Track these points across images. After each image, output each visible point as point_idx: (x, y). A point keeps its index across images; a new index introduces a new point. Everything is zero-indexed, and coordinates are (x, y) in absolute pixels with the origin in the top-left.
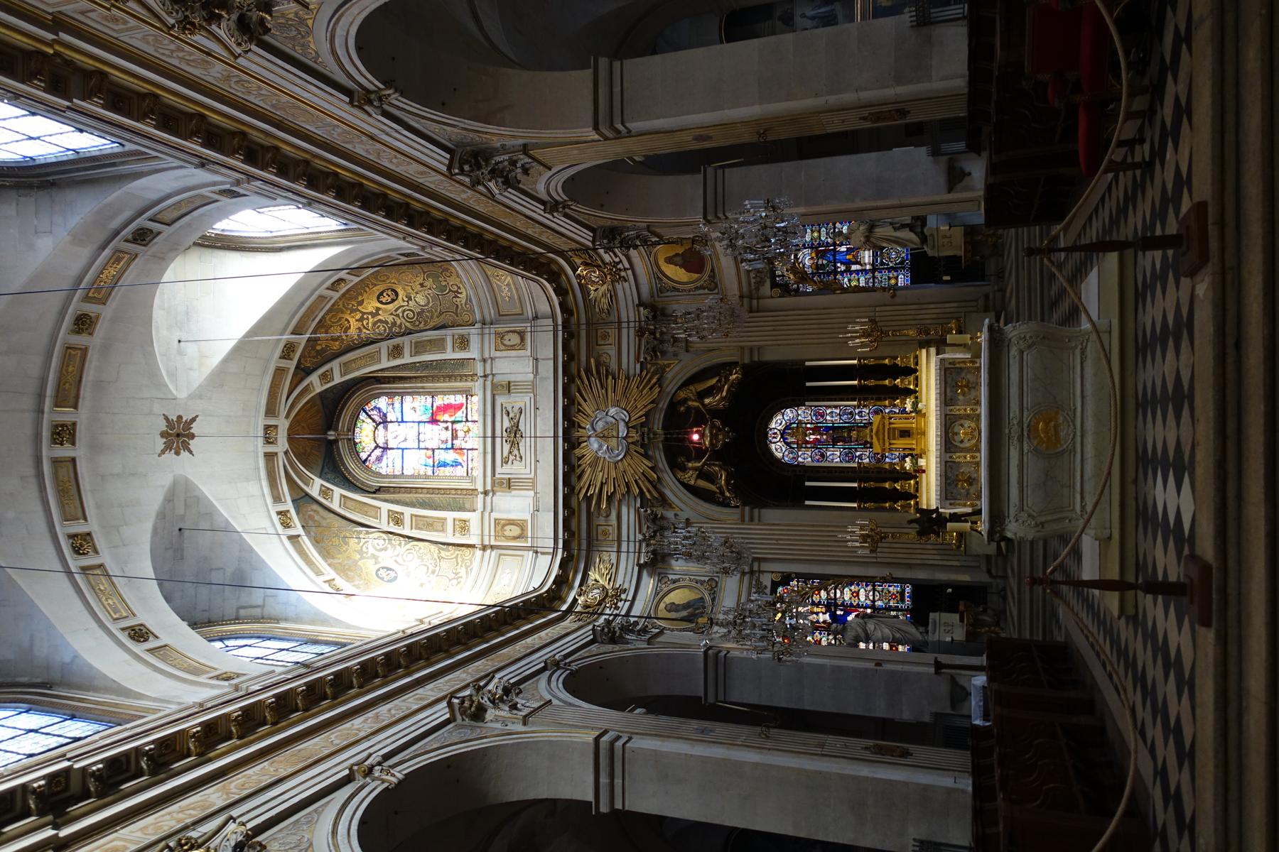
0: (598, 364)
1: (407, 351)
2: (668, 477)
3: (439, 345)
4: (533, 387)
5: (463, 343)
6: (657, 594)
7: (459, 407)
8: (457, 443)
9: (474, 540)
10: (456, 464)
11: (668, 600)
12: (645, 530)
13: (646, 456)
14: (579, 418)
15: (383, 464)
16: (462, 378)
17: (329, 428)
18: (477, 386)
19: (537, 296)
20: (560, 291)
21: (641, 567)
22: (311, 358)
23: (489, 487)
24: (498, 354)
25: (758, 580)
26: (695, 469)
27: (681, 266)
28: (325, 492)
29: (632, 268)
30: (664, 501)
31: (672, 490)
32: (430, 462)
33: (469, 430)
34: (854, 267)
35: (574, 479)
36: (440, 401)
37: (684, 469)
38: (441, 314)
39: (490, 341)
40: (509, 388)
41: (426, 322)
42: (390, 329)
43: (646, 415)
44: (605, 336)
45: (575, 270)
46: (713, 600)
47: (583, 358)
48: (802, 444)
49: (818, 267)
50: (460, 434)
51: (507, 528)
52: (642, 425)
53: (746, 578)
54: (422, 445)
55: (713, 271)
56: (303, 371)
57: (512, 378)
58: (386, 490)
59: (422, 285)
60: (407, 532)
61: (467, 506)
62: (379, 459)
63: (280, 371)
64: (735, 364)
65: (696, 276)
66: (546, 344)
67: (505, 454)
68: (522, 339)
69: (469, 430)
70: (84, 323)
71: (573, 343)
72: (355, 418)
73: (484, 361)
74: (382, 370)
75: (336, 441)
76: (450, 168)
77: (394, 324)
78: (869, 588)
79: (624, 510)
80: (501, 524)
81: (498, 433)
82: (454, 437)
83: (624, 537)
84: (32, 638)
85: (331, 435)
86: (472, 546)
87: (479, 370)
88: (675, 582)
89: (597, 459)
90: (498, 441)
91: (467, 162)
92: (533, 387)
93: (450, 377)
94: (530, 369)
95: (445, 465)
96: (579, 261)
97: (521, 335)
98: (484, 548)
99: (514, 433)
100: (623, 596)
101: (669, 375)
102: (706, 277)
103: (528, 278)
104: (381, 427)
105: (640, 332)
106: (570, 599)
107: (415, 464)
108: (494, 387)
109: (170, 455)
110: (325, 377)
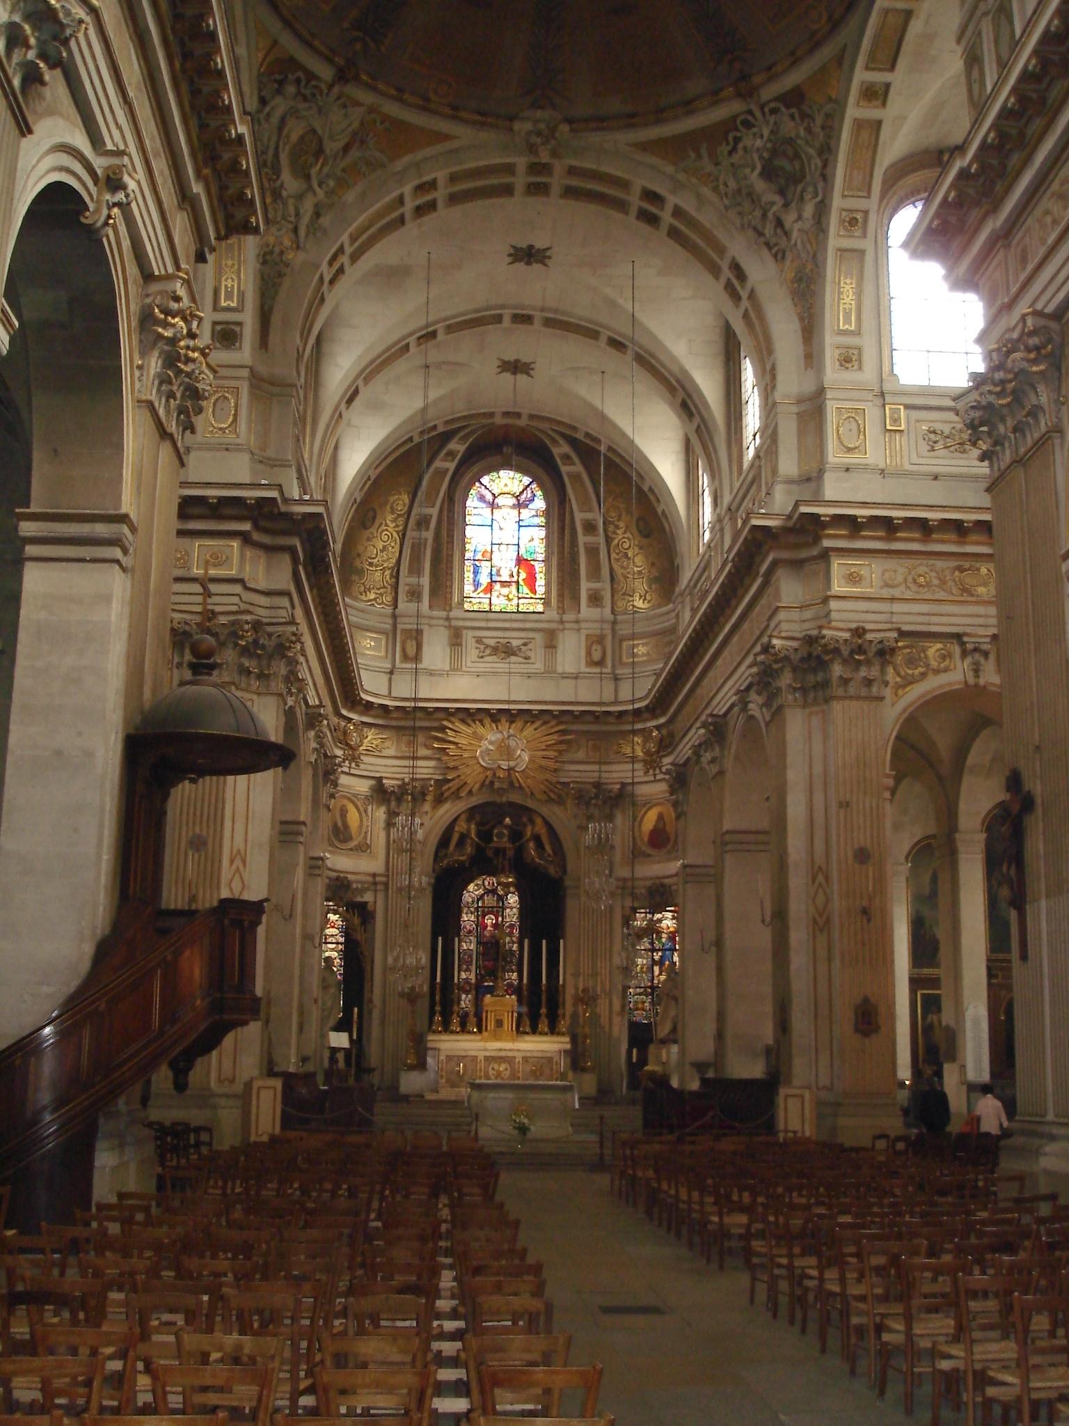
0: (569, 742)
1: (590, 539)
3: (595, 574)
5: (595, 599)
6: (355, 795)
9: (401, 605)
10: (477, 585)
13: (483, 785)
14: (519, 724)
15: (477, 503)
16: (561, 596)
18: (553, 614)
19: (638, 690)
20: (637, 713)
21: (380, 779)
22: (587, 451)
23: (454, 623)
24: (583, 638)
26: (469, 830)
27: (655, 826)
28: (451, 454)
29: (655, 781)
30: (439, 800)
32: (479, 556)
33: (509, 600)
34: (656, 969)
35: (461, 715)
36: (539, 567)
37: (469, 821)
39: (594, 629)
40: (551, 646)
41: (618, 560)
42: (612, 523)
43: (521, 787)
44: (596, 748)
45: (657, 727)
46: (351, 849)
47: (575, 727)
48: (482, 912)
50: (505, 591)
52: (511, 784)
53: (370, 879)
55: (649, 855)
56: (573, 442)
57: (559, 651)
58: (451, 510)
60: (408, 533)
62: (482, 498)
63: (574, 429)
64: (565, 872)
65: (646, 839)
66: (589, 694)
67: (486, 641)
69: (509, 600)
70: (617, 345)
71: (589, 718)
72: (525, 472)
73: (577, 622)
74: (572, 512)
75: (501, 452)
77: (617, 527)
79: (432, 763)
80: (417, 636)
81: (507, 634)
82: (505, 584)
85: (507, 450)
86: (396, 607)
88: (366, 811)
89: (480, 739)
90: (499, 634)
92: (549, 672)
93: (561, 584)
94: (565, 678)
95: (476, 573)
96: (664, 732)
97: (600, 663)
98: (394, 616)
99: (506, 651)
100: (353, 765)
101: (557, 810)
102: (644, 848)
104: (514, 501)
105: (597, 785)
106: (351, 715)
107: (476, 537)
110: (566, 458)
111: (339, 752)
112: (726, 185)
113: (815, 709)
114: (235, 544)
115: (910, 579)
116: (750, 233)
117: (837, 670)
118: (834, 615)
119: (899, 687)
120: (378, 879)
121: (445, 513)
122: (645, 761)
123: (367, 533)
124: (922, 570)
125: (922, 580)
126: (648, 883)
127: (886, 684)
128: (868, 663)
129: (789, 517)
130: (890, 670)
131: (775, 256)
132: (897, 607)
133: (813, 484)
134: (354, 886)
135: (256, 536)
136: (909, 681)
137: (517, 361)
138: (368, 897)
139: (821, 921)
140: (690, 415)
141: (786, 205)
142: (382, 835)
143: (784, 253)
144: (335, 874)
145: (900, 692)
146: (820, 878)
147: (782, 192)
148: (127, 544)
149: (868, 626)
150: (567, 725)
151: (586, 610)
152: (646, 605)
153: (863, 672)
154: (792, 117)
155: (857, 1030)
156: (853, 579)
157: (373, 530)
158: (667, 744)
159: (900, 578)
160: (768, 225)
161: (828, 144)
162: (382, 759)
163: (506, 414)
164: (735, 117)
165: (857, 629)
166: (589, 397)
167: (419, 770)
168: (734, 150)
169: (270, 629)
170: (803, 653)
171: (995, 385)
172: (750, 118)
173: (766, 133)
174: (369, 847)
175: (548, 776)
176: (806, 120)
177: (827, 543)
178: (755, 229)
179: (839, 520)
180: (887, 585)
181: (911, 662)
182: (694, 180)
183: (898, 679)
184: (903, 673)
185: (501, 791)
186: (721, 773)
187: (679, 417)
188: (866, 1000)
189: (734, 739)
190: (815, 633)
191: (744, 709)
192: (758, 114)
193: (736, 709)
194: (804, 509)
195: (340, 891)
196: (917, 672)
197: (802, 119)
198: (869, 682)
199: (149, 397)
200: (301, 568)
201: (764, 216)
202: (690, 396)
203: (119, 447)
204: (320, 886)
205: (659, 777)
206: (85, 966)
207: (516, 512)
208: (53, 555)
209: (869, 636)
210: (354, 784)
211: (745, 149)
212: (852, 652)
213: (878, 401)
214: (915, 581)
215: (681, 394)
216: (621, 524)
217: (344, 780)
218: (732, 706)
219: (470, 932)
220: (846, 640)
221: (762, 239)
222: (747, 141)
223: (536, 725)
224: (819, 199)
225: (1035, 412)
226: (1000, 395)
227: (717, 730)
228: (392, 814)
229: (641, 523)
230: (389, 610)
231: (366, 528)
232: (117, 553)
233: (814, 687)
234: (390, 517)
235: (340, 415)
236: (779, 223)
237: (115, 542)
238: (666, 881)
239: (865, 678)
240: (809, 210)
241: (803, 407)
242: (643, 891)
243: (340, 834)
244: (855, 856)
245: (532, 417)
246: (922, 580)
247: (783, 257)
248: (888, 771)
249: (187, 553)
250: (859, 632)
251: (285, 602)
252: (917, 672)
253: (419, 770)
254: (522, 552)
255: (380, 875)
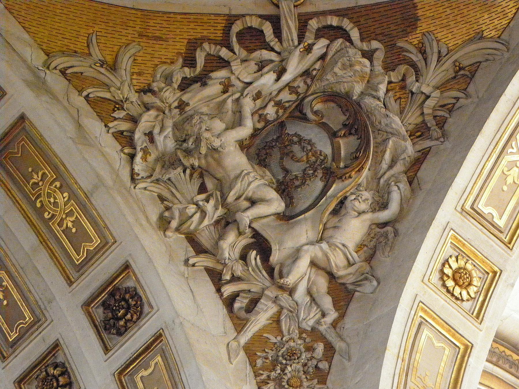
112: (150, 136)
116: (176, 239)
131: (229, 303)
141: (287, 217)
143: (254, 303)
147: (284, 189)
154: (369, 55)
160: (231, 237)
161: (441, 123)
164: (231, 19)
168: (202, 80)
172: (268, 29)
173: (294, 67)
176: (403, 68)
178: (192, 240)
182: (79, 101)
192: (290, 27)
197: (389, 67)
201: (226, 223)
211: (227, 87)
221: (203, 261)
222: (243, 72)
224: (384, 215)
236: (261, 245)
240: (354, 230)
247: (252, 306)
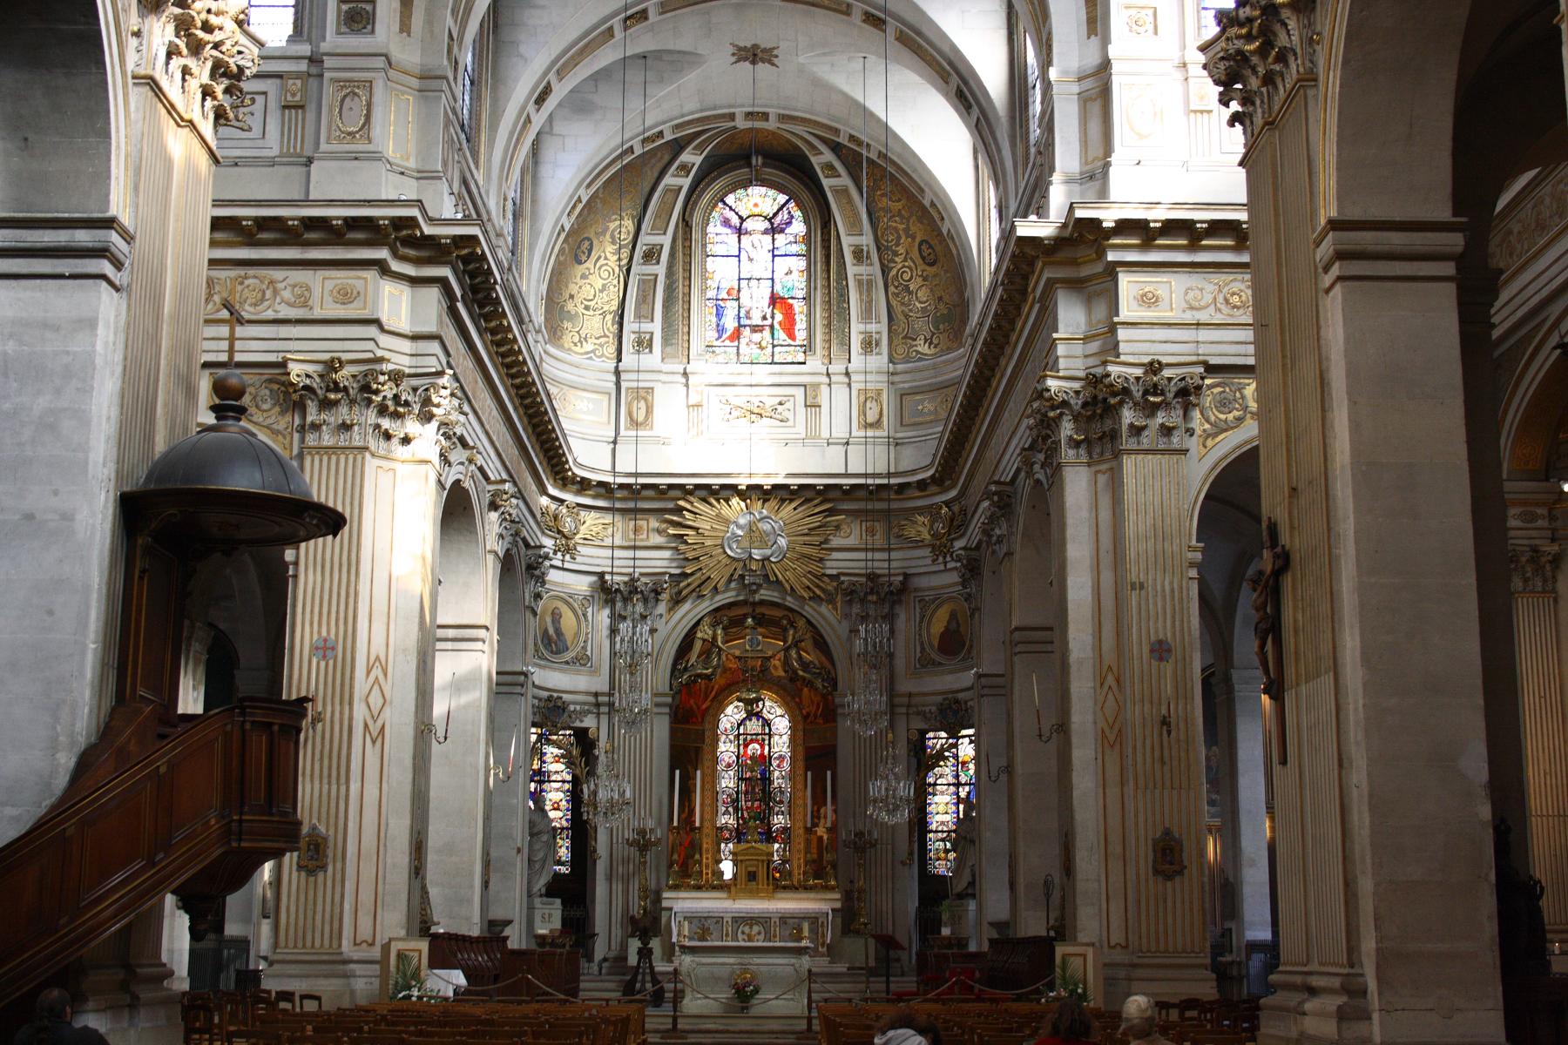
1: (862, 269)
2: (706, 606)
3: (867, 315)
4: (811, 437)
7: (792, 336)
8: (747, 332)
9: (628, 359)
11: (564, 609)
12: (644, 580)
14: (773, 503)
17: (765, 156)
20: (922, 485)
21: (601, 575)
22: (850, 156)
25: (590, 712)
26: (714, 637)
27: (947, 628)
28: (685, 169)
29: (946, 570)
30: (677, 601)
31: (690, 611)
32: (723, 295)
35: (703, 493)
37: (714, 626)
38: (907, 317)
41: (897, 295)
42: (887, 248)
43: (778, 581)
44: (872, 532)
45: (947, 503)
48: (743, 741)
49: (964, 763)
50: (757, 337)
51: (642, 404)
53: (591, 699)
54: (744, 283)
55: (940, 664)
56: (836, 148)
58: (688, 237)
59: (940, 299)
61: (668, 349)
62: (726, 222)
63: (837, 131)
68: (871, 425)
69: (762, 348)
70: (875, 21)
72: (781, 190)
76: (998, 483)
77: (896, 254)
78: (565, 824)
79: (667, 554)
80: (644, 395)
82: (756, 329)
83: (640, 554)
84: (543, 7)
85: (757, 161)
86: (619, 360)
87: (838, 367)
91: (1001, 499)
92: (811, 437)
95: (719, 315)
96: (956, 508)
97: (877, 424)
98: (617, 373)
100: (568, 557)
101: (824, 609)
102: (933, 655)
103: (940, 439)
104: (767, 225)
107: (720, 271)
108: (816, 386)
109: (732, 50)
110: (829, 166)
111: (548, 543)
113: (1104, 467)
114: (371, 274)
115: (1220, 299)
117: (1128, 416)
118: (1123, 347)
119: (1208, 435)
120: (601, 699)
121: (680, 242)
122: (933, 546)
123: (580, 269)
124: (1236, 286)
125: (1235, 299)
126: (939, 699)
127: (1190, 432)
128: (1166, 405)
129: (1065, 225)
130: (1196, 414)
132: (1204, 335)
133: (1096, 184)
134: (572, 708)
135: (395, 266)
136: (1220, 429)
137: (755, 46)
138: (589, 722)
139: (1112, 738)
140: (968, 107)
142: (607, 643)
144: (545, 694)
145: (1210, 443)
146: (1110, 680)
148: (121, 257)
149: (1164, 360)
150: (821, 499)
151: (857, 361)
152: (933, 351)
153: (1160, 418)
155: (1156, 872)
156: (1148, 300)
157: (590, 264)
158: (957, 524)
159: (1208, 298)
162: (600, 546)
163: (749, 115)
165: (1151, 364)
166: (847, 89)
167: (638, 563)
169: (415, 382)
170: (1087, 394)
171: (1241, 25)
174: (589, 659)
175: (813, 567)
177: (1111, 256)
179: (1126, 227)
180: (1192, 308)
181: (1223, 405)
183: (1207, 426)
184: (1213, 419)
185: (752, 589)
186: (1009, 554)
187: (957, 110)
188: (1167, 832)
189: (1021, 510)
190: (1099, 371)
191: (1030, 473)
193: (1023, 474)
194: (1079, 214)
195: (551, 713)
196: (1230, 416)
198: (1167, 431)
199: (149, 72)
200: (460, 305)
202: (966, 83)
203: (106, 134)
204: (524, 708)
205: (949, 566)
206: (62, 781)
207: (769, 238)
208: (25, 270)
209: (1167, 373)
210: (566, 581)
212: (1146, 393)
213: (1179, 75)
214: (1227, 301)
215: (955, 79)
216: (901, 250)
217: (553, 576)
218: (1018, 471)
219: (729, 765)
220: (1138, 379)
223: (794, 505)
225: (1282, 58)
226: (1249, 38)
227: (1004, 503)
228: (617, 618)
229: (924, 247)
230: (612, 365)
231: (580, 263)
232: (106, 267)
233: (1100, 439)
234: (610, 248)
235: (528, 120)
237: (101, 252)
238: (960, 696)
239: (1162, 425)
241: (1088, 84)
242: (934, 709)
243: (552, 645)
244: (1152, 651)
245: (783, 118)
246: (1235, 299)
248: (1194, 542)
249: (308, 289)
250: (1154, 367)
251: (435, 347)
252: (1230, 416)
253: (638, 563)
254: (778, 288)
255: (603, 694)
